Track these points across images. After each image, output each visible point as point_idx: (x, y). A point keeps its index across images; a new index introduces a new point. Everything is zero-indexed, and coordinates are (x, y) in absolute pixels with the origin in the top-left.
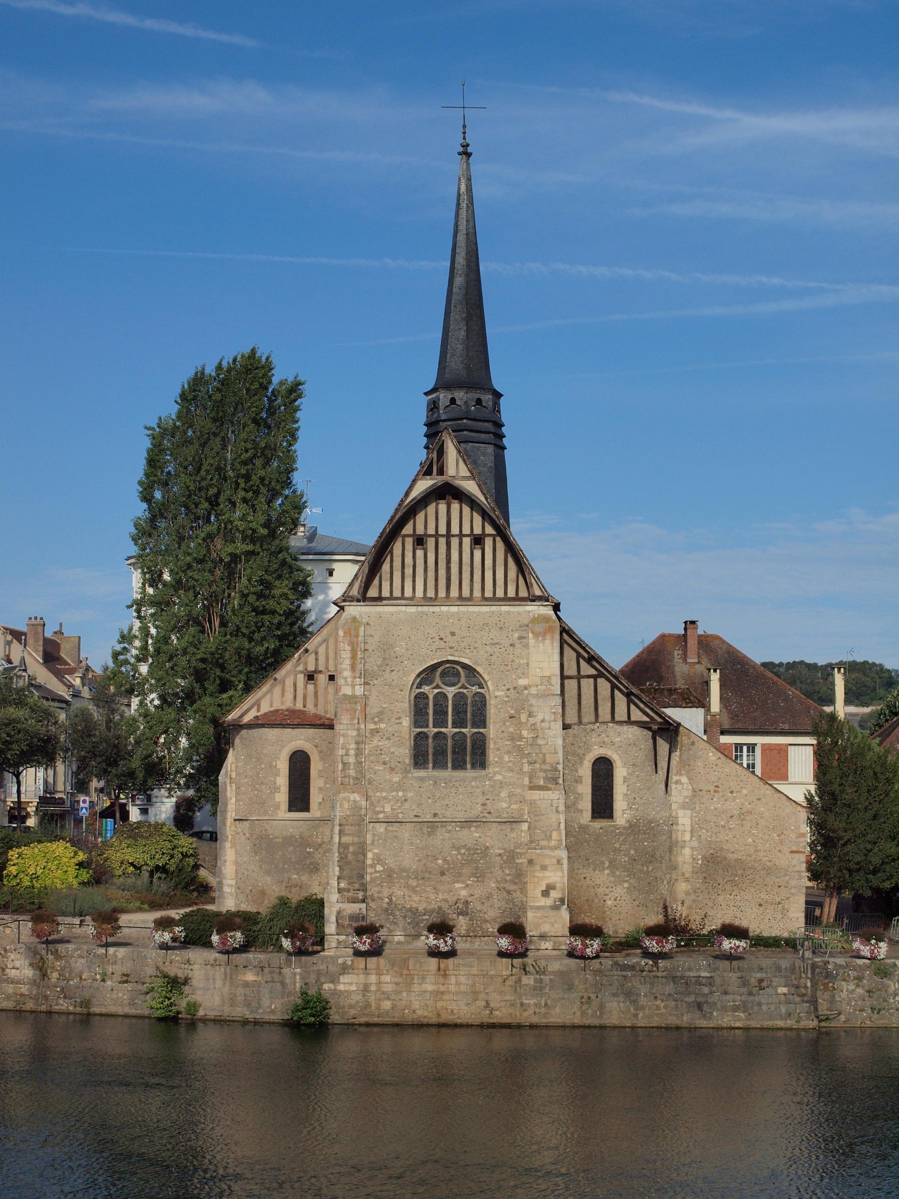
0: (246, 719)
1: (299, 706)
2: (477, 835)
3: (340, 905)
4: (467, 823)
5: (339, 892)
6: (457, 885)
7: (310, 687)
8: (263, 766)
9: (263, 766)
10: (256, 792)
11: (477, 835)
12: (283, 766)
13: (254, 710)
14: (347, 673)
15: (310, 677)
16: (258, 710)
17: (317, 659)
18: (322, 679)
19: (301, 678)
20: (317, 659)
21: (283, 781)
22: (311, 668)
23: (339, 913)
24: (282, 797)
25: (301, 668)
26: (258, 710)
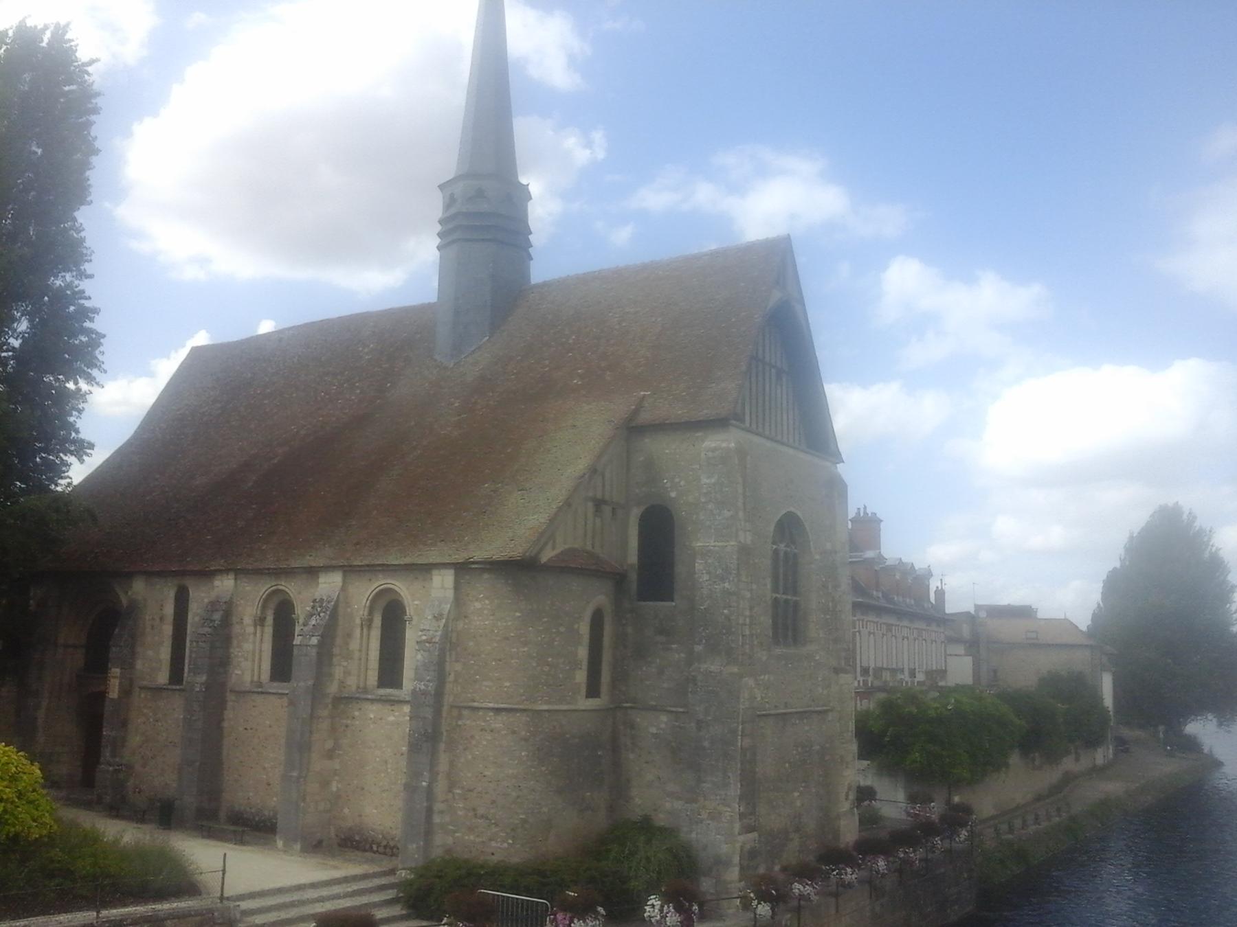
0: (545, 558)
1: (589, 548)
2: (807, 728)
3: (741, 838)
4: (802, 715)
5: (740, 819)
6: (796, 794)
7: (598, 520)
8: (562, 629)
9: (562, 629)
10: (546, 669)
11: (807, 728)
12: (584, 629)
13: (549, 547)
14: (741, 514)
15: (599, 504)
16: (553, 548)
17: (604, 486)
18: (607, 510)
19: (590, 504)
20: (604, 486)
21: (583, 653)
22: (599, 496)
23: (742, 847)
24: (581, 676)
25: (591, 494)
26: (553, 548)
